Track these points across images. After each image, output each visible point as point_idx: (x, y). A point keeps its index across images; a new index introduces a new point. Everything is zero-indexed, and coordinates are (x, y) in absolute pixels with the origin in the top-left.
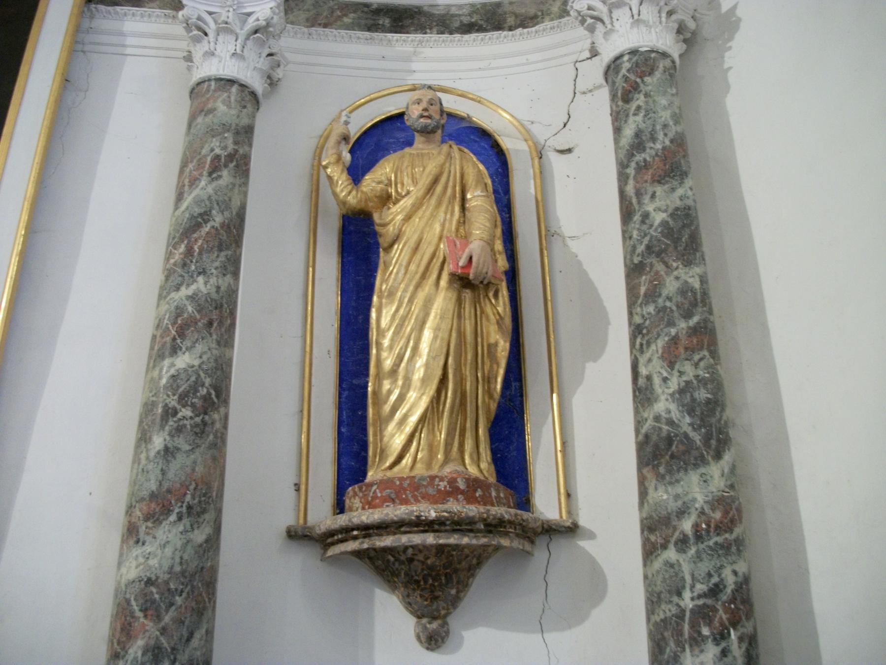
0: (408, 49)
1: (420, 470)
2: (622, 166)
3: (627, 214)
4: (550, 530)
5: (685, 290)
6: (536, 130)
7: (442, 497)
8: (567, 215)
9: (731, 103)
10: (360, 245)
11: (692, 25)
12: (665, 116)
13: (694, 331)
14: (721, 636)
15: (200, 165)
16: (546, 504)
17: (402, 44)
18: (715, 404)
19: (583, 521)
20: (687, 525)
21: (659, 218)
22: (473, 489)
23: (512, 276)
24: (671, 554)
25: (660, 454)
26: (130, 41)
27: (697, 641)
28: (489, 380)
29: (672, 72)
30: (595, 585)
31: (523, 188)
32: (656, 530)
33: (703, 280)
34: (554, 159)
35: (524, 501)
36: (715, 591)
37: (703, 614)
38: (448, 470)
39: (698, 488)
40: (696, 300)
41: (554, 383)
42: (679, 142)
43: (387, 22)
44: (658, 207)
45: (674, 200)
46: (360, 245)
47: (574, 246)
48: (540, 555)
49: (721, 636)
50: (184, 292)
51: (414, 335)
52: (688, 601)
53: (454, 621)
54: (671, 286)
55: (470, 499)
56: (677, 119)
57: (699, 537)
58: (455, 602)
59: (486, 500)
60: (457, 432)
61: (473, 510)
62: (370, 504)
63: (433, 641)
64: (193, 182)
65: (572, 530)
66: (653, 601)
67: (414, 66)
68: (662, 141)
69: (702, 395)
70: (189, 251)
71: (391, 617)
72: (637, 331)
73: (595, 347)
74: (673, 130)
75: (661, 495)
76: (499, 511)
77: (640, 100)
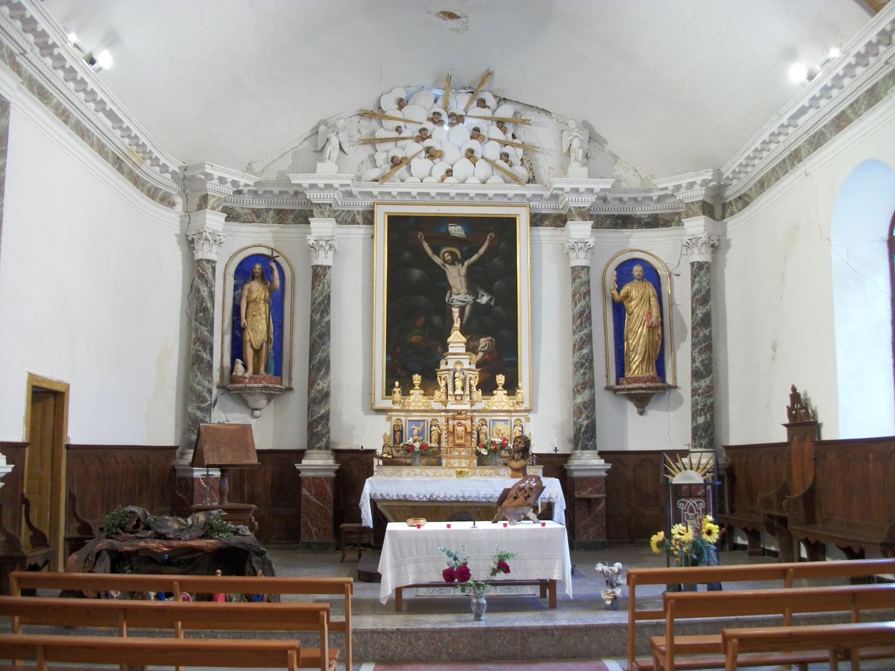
0: (628, 234)
1: (640, 375)
2: (693, 297)
3: (693, 312)
4: (670, 387)
5: (705, 336)
6: (669, 266)
7: (645, 382)
8: (678, 299)
9: (726, 270)
10: (619, 310)
11: (717, 244)
12: (705, 284)
13: (706, 346)
14: (705, 414)
15: (580, 295)
16: (669, 381)
17: (626, 232)
18: (710, 363)
19: (679, 384)
20: (700, 391)
21: (700, 315)
22: (652, 379)
23: (662, 323)
24: (696, 397)
25: (696, 375)
26: (543, 238)
27: (700, 415)
28: (656, 350)
29: (708, 269)
30: (680, 400)
31: (666, 289)
32: (694, 392)
33: (710, 332)
34: (674, 277)
35: (663, 380)
36: (705, 405)
37: (702, 410)
38: (647, 374)
39: (704, 383)
40: (708, 338)
41: (673, 350)
42: (708, 292)
43: (620, 222)
44: (700, 313)
45: (705, 311)
46: (619, 310)
47: (679, 307)
48: (668, 393)
49: (705, 414)
50: (582, 333)
51: (637, 337)
52: (699, 407)
53: (646, 409)
54: (701, 335)
55: (652, 382)
56: (708, 284)
57: (703, 393)
58: (647, 404)
59: (656, 382)
60: (648, 365)
61: (653, 385)
62: (629, 383)
63: (641, 413)
64: (579, 301)
65: (676, 387)
66: (693, 406)
67: (631, 240)
68: (704, 292)
69: (706, 362)
70: (582, 322)
71: (631, 408)
72: (693, 344)
73: (683, 339)
74: (707, 287)
75: (695, 384)
76: (659, 384)
77: (698, 279)
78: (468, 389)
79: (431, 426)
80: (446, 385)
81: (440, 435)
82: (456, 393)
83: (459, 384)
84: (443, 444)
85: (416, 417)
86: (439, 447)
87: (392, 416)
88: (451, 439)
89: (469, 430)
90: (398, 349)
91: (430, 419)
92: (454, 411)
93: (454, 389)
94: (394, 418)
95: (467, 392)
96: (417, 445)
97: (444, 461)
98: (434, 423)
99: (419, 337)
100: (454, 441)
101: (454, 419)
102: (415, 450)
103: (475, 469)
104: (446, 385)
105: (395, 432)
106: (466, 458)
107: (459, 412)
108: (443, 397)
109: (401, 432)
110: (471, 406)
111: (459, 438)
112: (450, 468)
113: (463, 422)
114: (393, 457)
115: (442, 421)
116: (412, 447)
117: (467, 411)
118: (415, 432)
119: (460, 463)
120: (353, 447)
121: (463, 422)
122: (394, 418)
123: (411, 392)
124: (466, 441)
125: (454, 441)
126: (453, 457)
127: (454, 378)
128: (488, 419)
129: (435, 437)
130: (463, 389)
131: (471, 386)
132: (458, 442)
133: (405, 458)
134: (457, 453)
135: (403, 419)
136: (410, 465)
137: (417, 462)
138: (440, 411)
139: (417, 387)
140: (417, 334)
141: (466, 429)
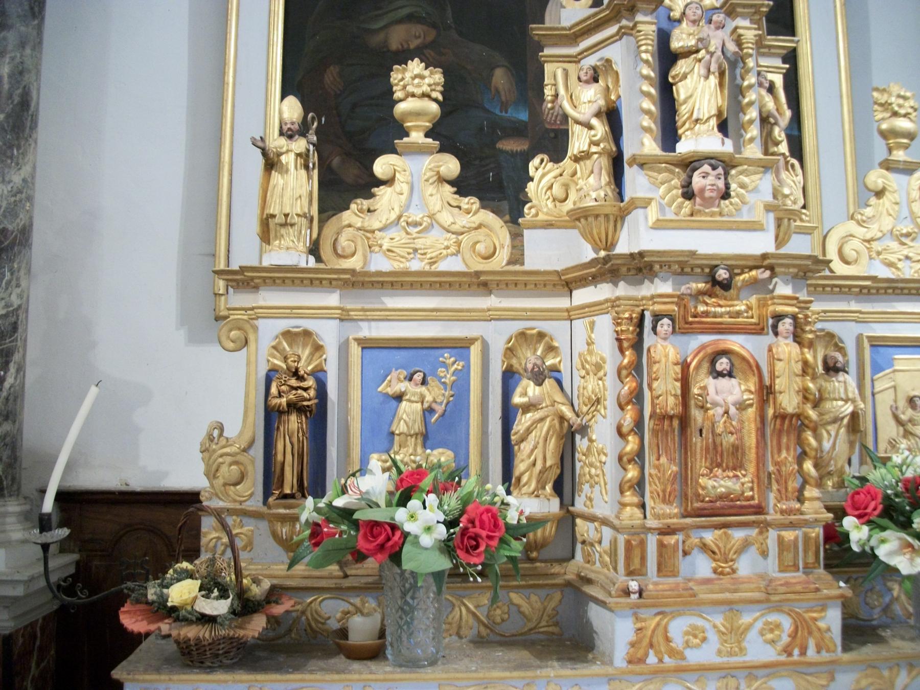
78: (754, 131)
79: (509, 377)
80: (612, 116)
81: (569, 436)
82: (684, 147)
83: (699, 92)
84: (599, 497)
85: (409, 318)
86: (568, 519)
87: (256, 315)
88: (662, 466)
89: (789, 402)
90: (331, 76)
91: (498, 336)
92: (682, 265)
93: (669, 134)
94: (269, 330)
95: (753, 151)
96: (424, 522)
97: (617, 631)
98: (529, 358)
99: (418, 29)
100: (685, 477)
101: (684, 326)
102: (411, 560)
103: (831, 669)
104: (612, 116)
105: (272, 417)
106: (769, 597)
107: (718, 279)
108: (592, 185)
109: (316, 415)
110: (780, 241)
111: (728, 458)
112: (660, 673)
113: (736, 342)
114: (246, 607)
115: (588, 340)
116: (387, 541)
117: (763, 262)
118: (408, 414)
119: (735, 635)
120: (138, 483)
121: (736, 342)
122: (269, 330)
123: (382, 166)
124: (763, 480)
125: (685, 477)
126: (688, 600)
127: (667, 57)
128: (847, 333)
129: (536, 451)
130: (723, 127)
131: (765, 120)
132: (718, 484)
133: (338, 591)
134: (703, 566)
135: (328, 332)
136: (373, 653)
137: (423, 638)
138: (568, 282)
139: (417, 137)
140: (410, 18)
141: (766, 393)
